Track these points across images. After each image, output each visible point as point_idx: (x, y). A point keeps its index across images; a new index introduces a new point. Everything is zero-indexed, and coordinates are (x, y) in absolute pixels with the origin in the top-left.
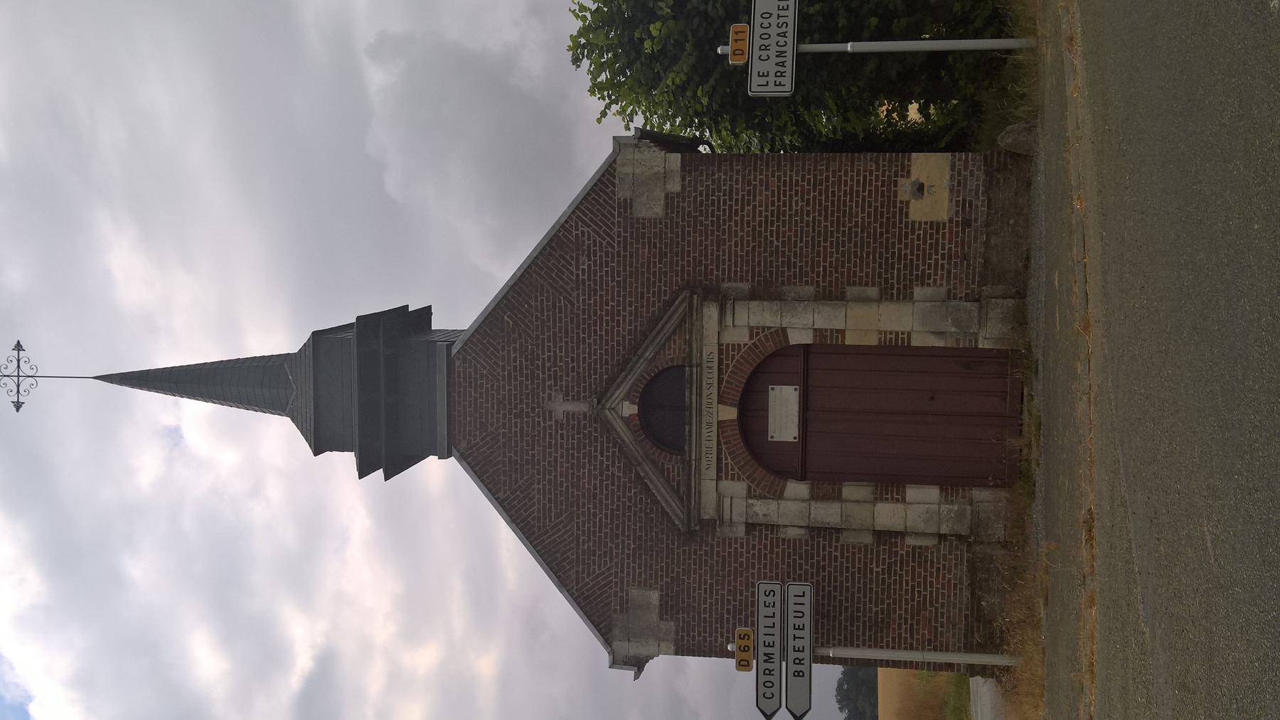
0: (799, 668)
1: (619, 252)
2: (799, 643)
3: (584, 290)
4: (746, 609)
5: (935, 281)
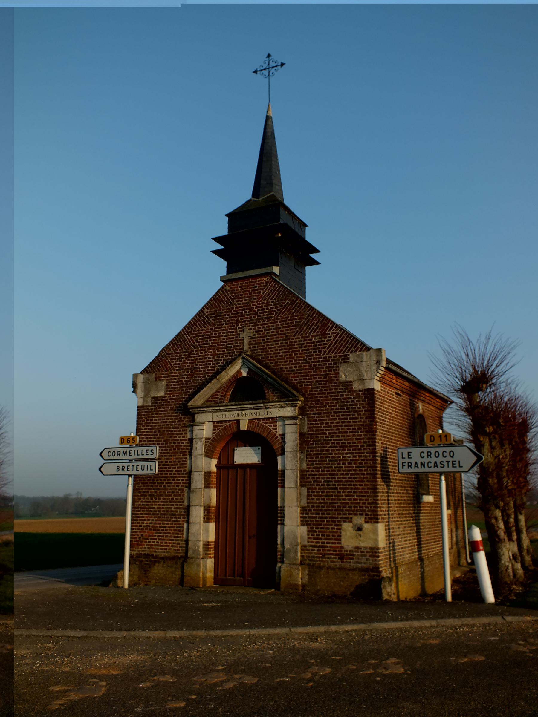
0: (121, 469)
1: (321, 358)
2: (131, 468)
3: (302, 341)
4: (156, 441)
5: (310, 538)
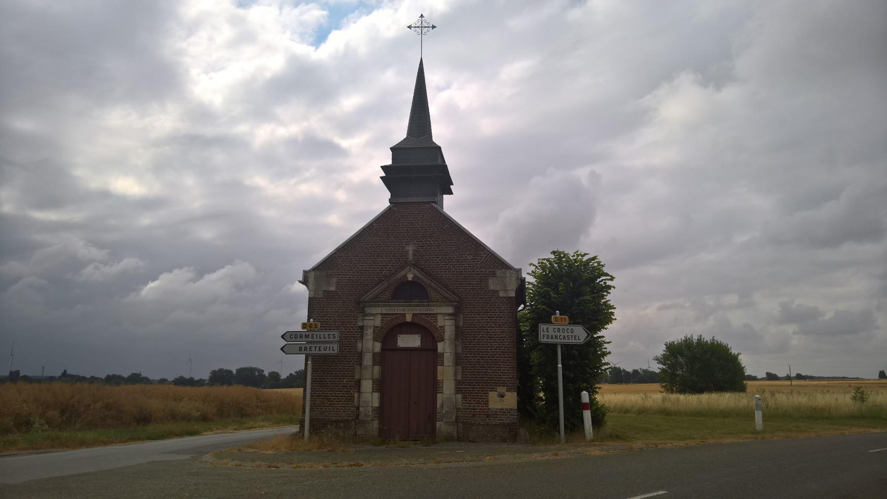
2: (313, 349)
